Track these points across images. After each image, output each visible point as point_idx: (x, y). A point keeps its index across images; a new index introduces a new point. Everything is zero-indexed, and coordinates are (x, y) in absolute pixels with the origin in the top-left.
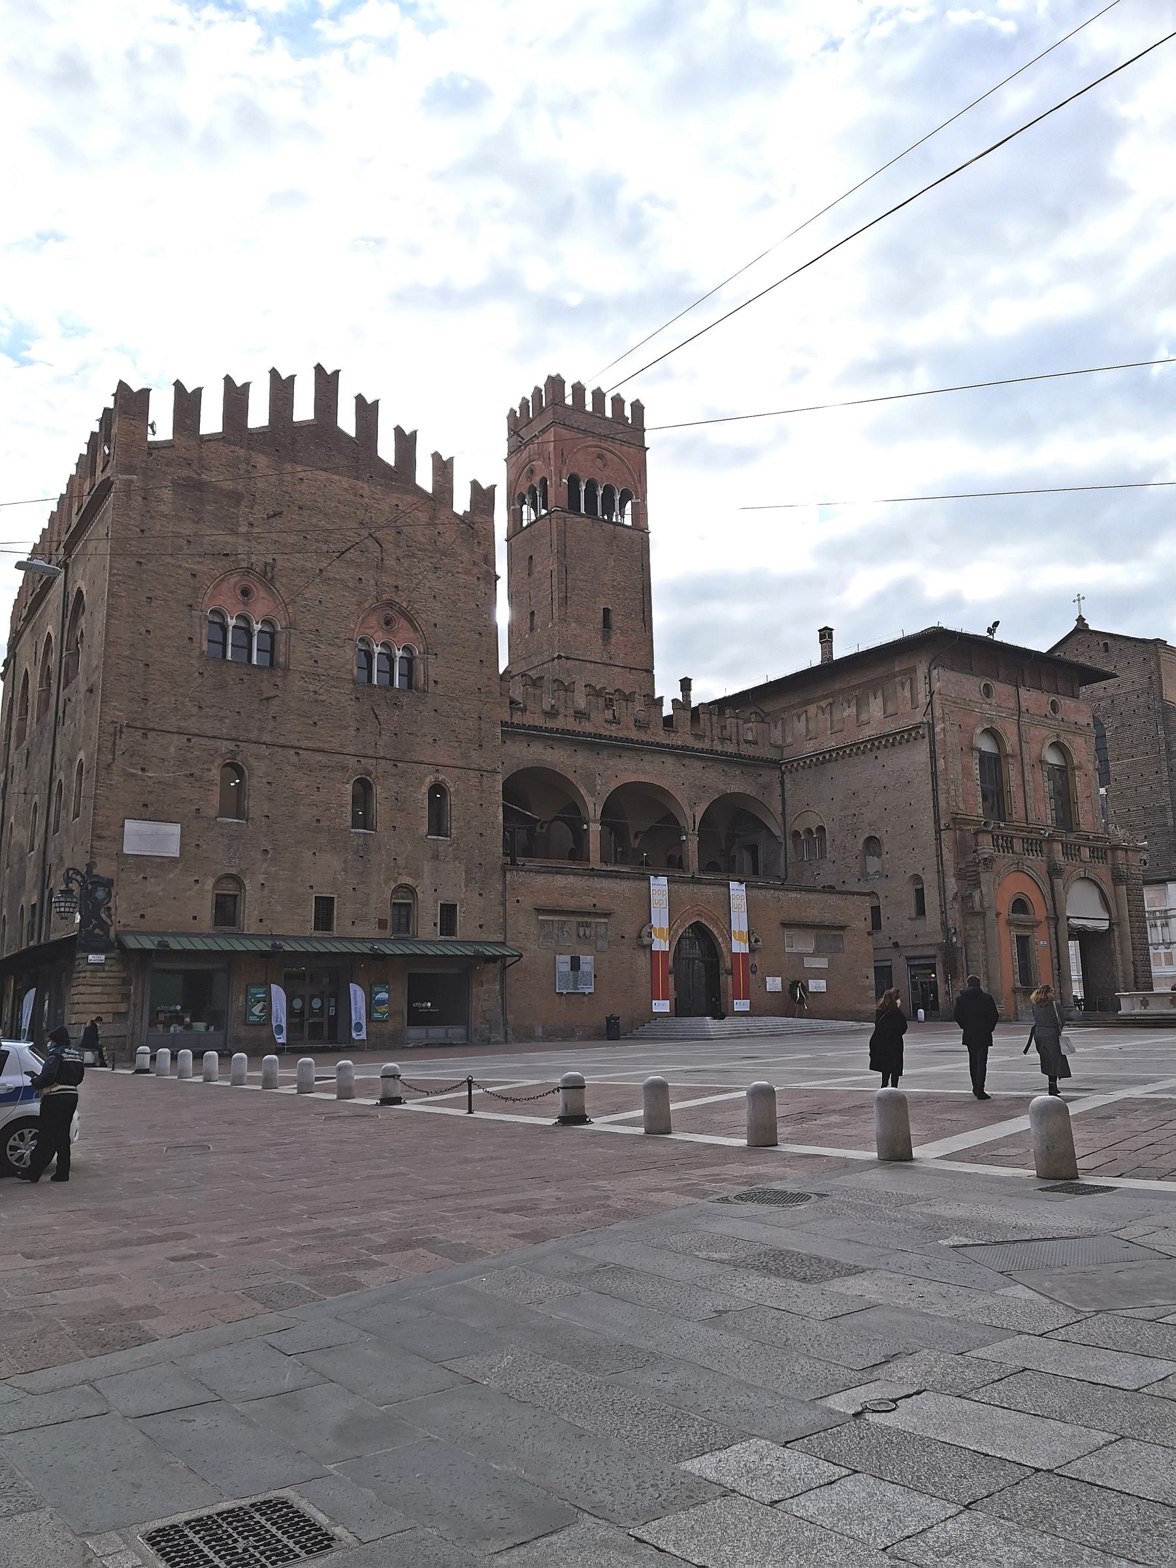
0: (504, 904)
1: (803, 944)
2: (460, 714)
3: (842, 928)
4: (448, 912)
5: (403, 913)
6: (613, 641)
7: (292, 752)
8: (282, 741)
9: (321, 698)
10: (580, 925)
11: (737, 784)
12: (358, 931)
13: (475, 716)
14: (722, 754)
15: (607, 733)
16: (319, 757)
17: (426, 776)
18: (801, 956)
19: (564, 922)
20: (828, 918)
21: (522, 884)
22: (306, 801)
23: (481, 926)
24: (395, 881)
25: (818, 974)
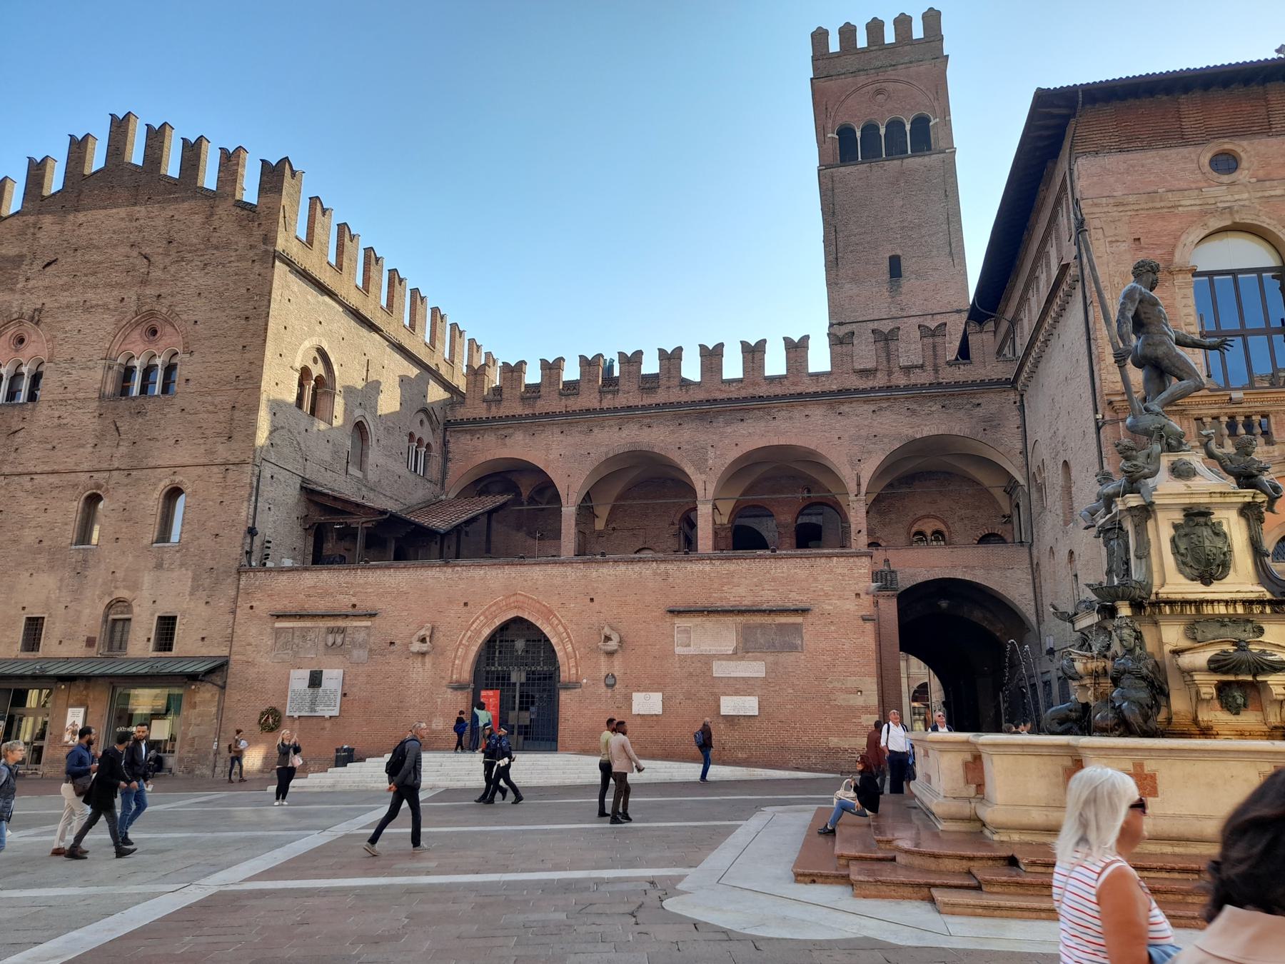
0: (234, 612)
1: (712, 641)
2: (211, 408)
3: (804, 611)
4: (167, 626)
5: (116, 626)
6: (904, 290)
7: (28, 478)
8: (20, 469)
9: (65, 421)
10: (331, 631)
11: (932, 423)
12: (64, 652)
13: (229, 406)
14: (906, 388)
15: (724, 396)
16: (53, 479)
17: (161, 480)
18: (707, 660)
19: (309, 629)
20: (769, 597)
21: (258, 587)
22: (33, 524)
23: (203, 639)
24: (110, 595)
25: (741, 687)
